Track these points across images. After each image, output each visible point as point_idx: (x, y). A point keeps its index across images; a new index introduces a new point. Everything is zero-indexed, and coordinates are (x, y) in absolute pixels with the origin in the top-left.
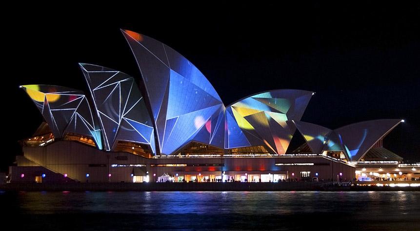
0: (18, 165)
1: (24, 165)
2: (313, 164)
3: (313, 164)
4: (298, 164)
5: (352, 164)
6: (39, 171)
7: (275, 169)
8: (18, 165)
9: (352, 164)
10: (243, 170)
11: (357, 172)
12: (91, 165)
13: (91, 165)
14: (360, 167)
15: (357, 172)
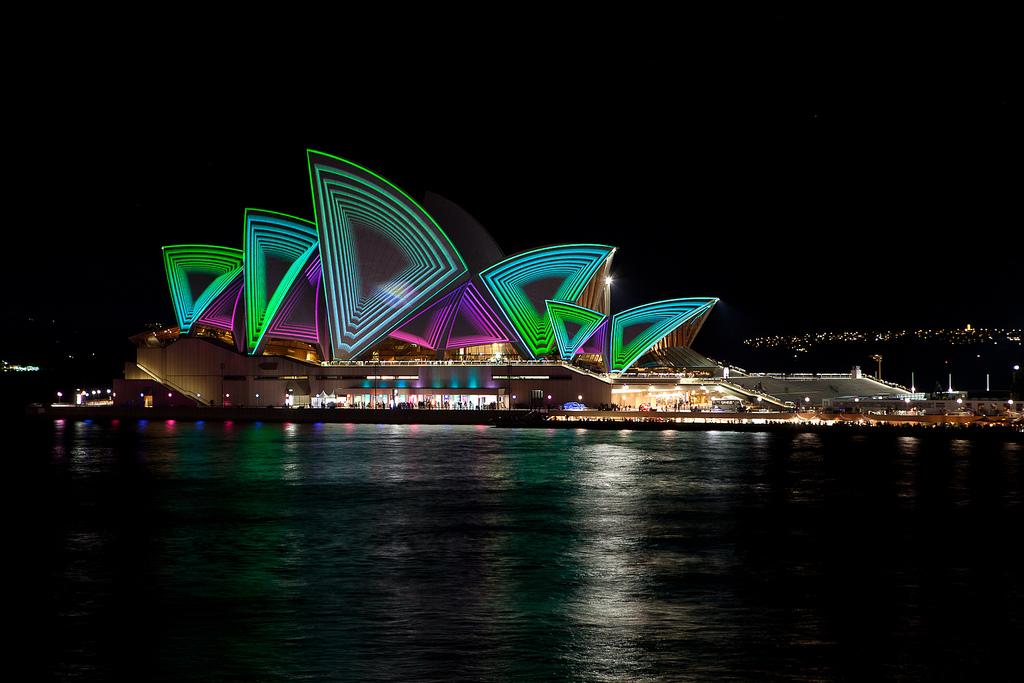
0: (126, 378)
1: (134, 378)
2: (547, 377)
3: (547, 377)
4: (527, 377)
5: (608, 378)
6: (150, 387)
7: (492, 386)
8: (126, 378)
9: (608, 378)
10: (446, 389)
11: (614, 391)
12: (227, 378)
13: (227, 378)
14: (619, 383)
15: (614, 391)
